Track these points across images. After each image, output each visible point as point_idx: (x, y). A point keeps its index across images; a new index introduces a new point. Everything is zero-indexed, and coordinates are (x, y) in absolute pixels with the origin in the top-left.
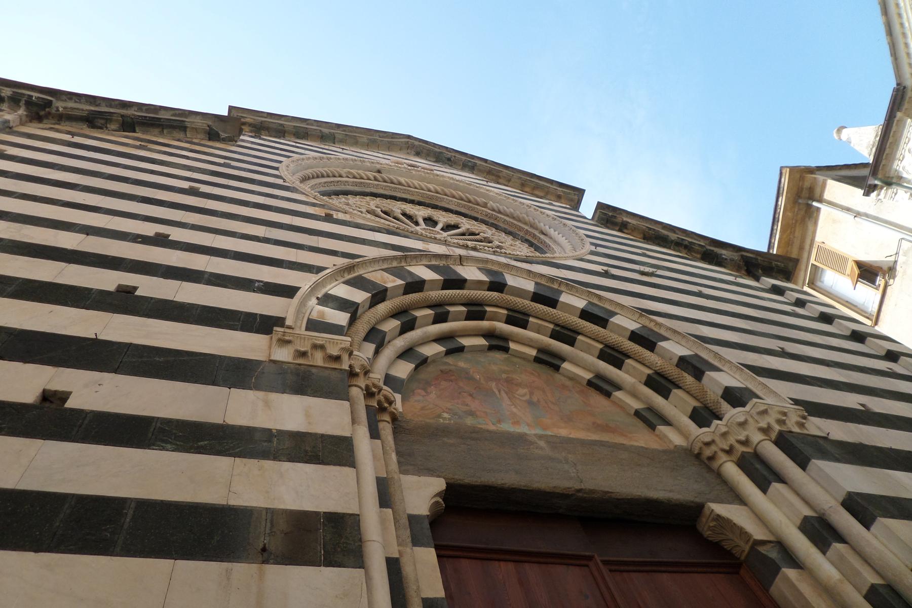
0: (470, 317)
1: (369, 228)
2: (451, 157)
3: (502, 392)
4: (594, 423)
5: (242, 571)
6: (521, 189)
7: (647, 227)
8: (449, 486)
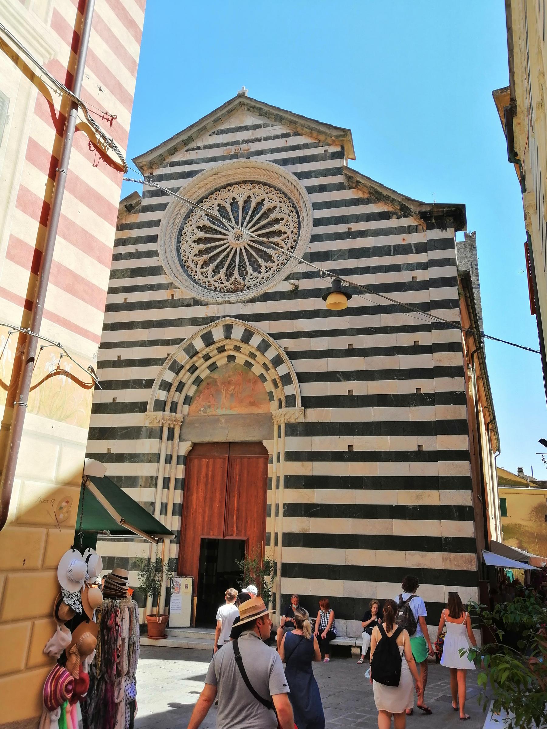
1: (185, 303)
2: (267, 112)
3: (224, 391)
4: (250, 402)
6: (310, 135)
7: (371, 186)
8: (192, 443)
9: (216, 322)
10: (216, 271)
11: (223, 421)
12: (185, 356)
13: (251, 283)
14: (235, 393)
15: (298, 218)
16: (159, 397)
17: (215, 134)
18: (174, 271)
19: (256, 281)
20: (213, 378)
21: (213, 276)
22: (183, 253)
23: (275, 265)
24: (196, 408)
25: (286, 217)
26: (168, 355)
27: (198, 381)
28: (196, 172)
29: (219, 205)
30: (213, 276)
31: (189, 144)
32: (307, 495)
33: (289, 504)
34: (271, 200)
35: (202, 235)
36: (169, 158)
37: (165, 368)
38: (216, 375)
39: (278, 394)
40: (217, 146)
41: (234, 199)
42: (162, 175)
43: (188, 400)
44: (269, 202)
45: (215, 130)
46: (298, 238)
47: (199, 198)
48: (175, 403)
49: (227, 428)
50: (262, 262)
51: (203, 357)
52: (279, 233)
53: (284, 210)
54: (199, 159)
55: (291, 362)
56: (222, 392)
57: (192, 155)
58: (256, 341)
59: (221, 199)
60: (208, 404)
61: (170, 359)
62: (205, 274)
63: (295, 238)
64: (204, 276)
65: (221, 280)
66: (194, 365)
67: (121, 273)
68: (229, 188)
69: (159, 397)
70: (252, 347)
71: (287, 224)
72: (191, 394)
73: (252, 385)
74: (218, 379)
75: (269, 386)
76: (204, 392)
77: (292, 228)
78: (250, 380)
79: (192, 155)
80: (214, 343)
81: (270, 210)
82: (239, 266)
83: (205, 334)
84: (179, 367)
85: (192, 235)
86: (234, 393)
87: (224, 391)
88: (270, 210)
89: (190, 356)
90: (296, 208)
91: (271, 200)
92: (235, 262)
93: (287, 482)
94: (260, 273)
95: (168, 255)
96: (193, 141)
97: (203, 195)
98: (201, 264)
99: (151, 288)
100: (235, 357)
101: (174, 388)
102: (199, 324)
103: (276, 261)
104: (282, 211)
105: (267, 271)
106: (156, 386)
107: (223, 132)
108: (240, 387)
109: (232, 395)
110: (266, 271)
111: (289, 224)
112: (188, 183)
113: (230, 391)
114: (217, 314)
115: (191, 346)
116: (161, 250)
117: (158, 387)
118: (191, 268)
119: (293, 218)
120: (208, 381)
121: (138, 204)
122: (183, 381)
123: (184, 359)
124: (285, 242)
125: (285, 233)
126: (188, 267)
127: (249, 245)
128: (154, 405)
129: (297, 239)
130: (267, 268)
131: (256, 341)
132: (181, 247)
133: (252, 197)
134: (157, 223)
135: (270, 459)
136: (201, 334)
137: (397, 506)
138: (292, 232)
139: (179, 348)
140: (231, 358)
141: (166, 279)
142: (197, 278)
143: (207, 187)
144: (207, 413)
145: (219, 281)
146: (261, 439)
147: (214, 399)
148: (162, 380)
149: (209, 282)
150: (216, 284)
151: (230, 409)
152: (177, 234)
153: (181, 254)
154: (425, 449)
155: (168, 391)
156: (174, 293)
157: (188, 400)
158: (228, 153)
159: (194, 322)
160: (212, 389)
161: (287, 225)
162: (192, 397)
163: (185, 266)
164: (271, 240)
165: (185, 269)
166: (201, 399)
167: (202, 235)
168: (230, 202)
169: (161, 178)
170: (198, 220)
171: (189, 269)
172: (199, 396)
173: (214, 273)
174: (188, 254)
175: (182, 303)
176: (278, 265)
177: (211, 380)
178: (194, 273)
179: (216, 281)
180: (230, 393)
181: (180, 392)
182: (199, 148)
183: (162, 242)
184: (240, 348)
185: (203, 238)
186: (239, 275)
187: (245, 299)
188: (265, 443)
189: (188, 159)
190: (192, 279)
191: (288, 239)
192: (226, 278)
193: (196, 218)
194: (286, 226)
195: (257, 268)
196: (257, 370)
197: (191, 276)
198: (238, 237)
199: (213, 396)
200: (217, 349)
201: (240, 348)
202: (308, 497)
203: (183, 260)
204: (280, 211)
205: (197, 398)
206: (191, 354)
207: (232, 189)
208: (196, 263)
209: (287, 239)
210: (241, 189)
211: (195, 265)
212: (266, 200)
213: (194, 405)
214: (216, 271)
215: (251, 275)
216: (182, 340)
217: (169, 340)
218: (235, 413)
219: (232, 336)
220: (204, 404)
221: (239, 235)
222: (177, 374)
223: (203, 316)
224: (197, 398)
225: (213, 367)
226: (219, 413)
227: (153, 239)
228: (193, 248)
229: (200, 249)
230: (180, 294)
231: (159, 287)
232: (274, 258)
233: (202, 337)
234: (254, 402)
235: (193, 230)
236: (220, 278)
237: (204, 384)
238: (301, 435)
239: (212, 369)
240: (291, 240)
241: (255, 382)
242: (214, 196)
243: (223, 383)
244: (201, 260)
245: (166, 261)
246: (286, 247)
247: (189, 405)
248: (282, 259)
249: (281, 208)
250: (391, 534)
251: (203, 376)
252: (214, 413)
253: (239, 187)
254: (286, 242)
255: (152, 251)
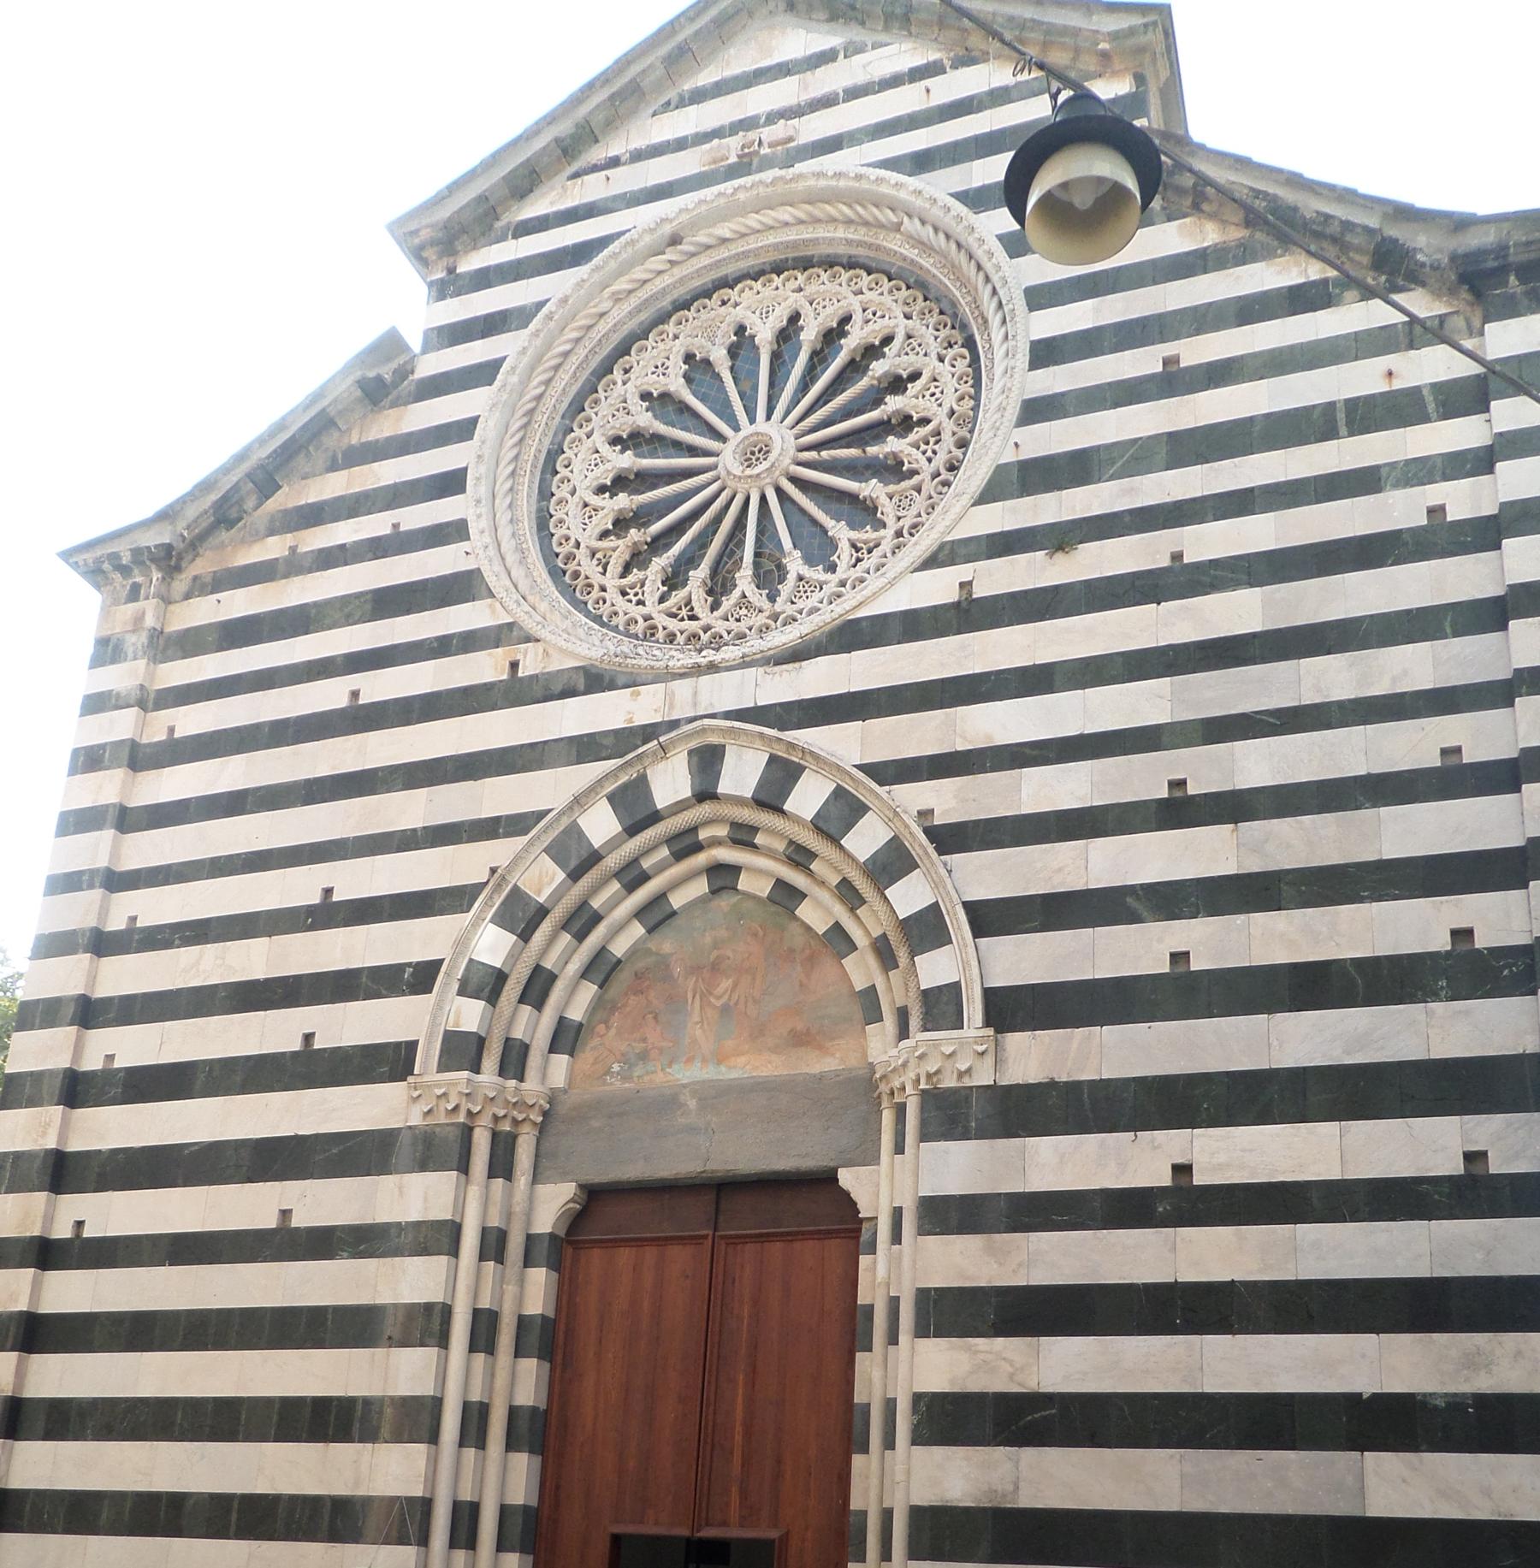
0: (679, 856)
3: (698, 997)
5: (379, 1352)
9: (661, 739)
10: (674, 580)
11: (692, 1104)
12: (550, 872)
13: (800, 604)
14: (736, 1004)
15: (975, 361)
16: (457, 1024)
17: (672, 106)
18: (524, 585)
19: (817, 596)
20: (657, 954)
21: (662, 600)
22: (559, 533)
23: (888, 533)
24: (593, 1064)
25: (930, 366)
26: (493, 871)
27: (601, 968)
28: (604, 242)
29: (689, 358)
30: (662, 600)
31: (580, 152)
32: (1004, 1359)
33: (934, 1394)
34: (874, 314)
35: (627, 460)
36: (513, 209)
37: (479, 919)
38: (666, 944)
39: (893, 992)
40: (680, 145)
41: (740, 330)
42: (488, 269)
43: (566, 1038)
44: (868, 321)
45: (672, 94)
46: (971, 431)
47: (616, 338)
48: (518, 1042)
49: (706, 1129)
50: (840, 531)
51: (617, 875)
52: (904, 424)
53: (920, 345)
54: (615, 198)
55: (945, 864)
56: (690, 1001)
57: (593, 188)
58: (807, 798)
59: (695, 333)
60: (639, 1047)
61: (499, 885)
62: (636, 594)
63: (963, 433)
64: (630, 601)
65: (692, 609)
66: (584, 905)
67: (341, 609)
68: (725, 293)
69: (457, 1024)
70: (797, 820)
71: (932, 390)
72: (576, 1014)
73: (799, 968)
74: (674, 958)
75: (861, 970)
76: (625, 1005)
77: (950, 400)
78: (792, 951)
79: (593, 188)
80: (655, 817)
81: (872, 352)
82: (757, 555)
83: (625, 788)
84: (532, 910)
85: (593, 467)
86: (732, 1003)
87: (698, 997)
88: (872, 352)
89: (568, 871)
90: (964, 327)
91: (874, 314)
92: (741, 543)
93: (928, 1312)
94: (832, 568)
95: (505, 533)
96: (597, 141)
97: (631, 325)
98: (621, 561)
99: (442, 647)
100: (735, 870)
101: (511, 991)
102: (604, 755)
103: (890, 520)
104: (913, 349)
105: (859, 560)
106: (446, 985)
107: (699, 96)
108: (754, 979)
109: (725, 1010)
110: (854, 560)
111: (940, 389)
112: (573, 281)
113: (719, 998)
114: (668, 716)
115: (575, 832)
116: (479, 516)
117: (456, 986)
118: (587, 578)
119: (954, 366)
120: (640, 965)
121: (404, 372)
122: (548, 964)
123: (549, 884)
124: (924, 453)
125: (925, 421)
126: (576, 575)
127: (794, 480)
128: (442, 1051)
129: (969, 436)
130: (857, 550)
131: (807, 798)
132: (553, 512)
133: (807, 312)
134: (463, 430)
135: (865, 1236)
136: (610, 788)
137: (1376, 1397)
138: (952, 413)
139: (531, 843)
140: (723, 876)
141: (493, 612)
142: (605, 610)
143: (643, 294)
144: (635, 1079)
145: (684, 613)
146: (832, 1164)
147: (658, 1028)
148: (471, 960)
149: (647, 618)
150: (673, 625)
151: (719, 1062)
152: (540, 466)
153: (552, 535)
154: (1496, 1166)
155: (493, 998)
156: (519, 657)
157: (566, 1038)
158: (715, 162)
159: (585, 748)
160: (652, 994)
161: (933, 395)
162: (581, 1025)
163: (564, 573)
164: (872, 450)
165: (564, 582)
166: (613, 1032)
167: (627, 460)
168: (728, 342)
169: (485, 279)
170: (614, 416)
171: (580, 582)
172: (606, 1022)
173: (665, 588)
174: (576, 534)
175: (547, 688)
176: (899, 534)
177: (651, 960)
178: (595, 594)
179: (674, 616)
180: (718, 1003)
181: (539, 1005)
182: (614, 162)
183: (483, 491)
184: (754, 830)
185: (632, 477)
186: (758, 587)
187: (772, 652)
188: (846, 1178)
189: (576, 203)
190: (588, 614)
191: (937, 442)
192: (710, 599)
193: (604, 409)
194: (928, 397)
195: (820, 551)
196: (817, 913)
197: (586, 603)
198: (757, 451)
199: (655, 1018)
200: (670, 840)
201: (754, 830)
202: (1011, 1370)
203: (557, 555)
204: (908, 349)
205: (601, 1028)
206: (573, 863)
207: (733, 294)
208: (604, 561)
209: (932, 440)
210: (768, 292)
211: (600, 569)
212: (858, 317)
213: (587, 1056)
214: (674, 580)
215: (801, 578)
216: (541, 815)
217: (496, 820)
218: (734, 1075)
219: (723, 787)
220: (623, 1047)
221: (756, 450)
222: (525, 936)
223: (619, 724)
224: (601, 1028)
225: (656, 915)
226: (678, 1076)
227: (451, 483)
228: (593, 513)
229: (620, 511)
230: (540, 657)
231: (469, 642)
232: (882, 514)
233: (611, 798)
234: (808, 1033)
235: (598, 452)
236: (688, 602)
237: (623, 978)
238: (981, 1135)
239: (652, 923)
240: (948, 440)
241: (811, 961)
242: (671, 328)
243: (695, 969)
244: (620, 549)
245: (492, 552)
246: (927, 470)
247: (571, 1054)
248: (914, 511)
249: (909, 337)
250: (1357, 1513)
251: (619, 948)
252: (659, 1078)
253: (758, 285)
254: (929, 453)
255: (448, 524)
